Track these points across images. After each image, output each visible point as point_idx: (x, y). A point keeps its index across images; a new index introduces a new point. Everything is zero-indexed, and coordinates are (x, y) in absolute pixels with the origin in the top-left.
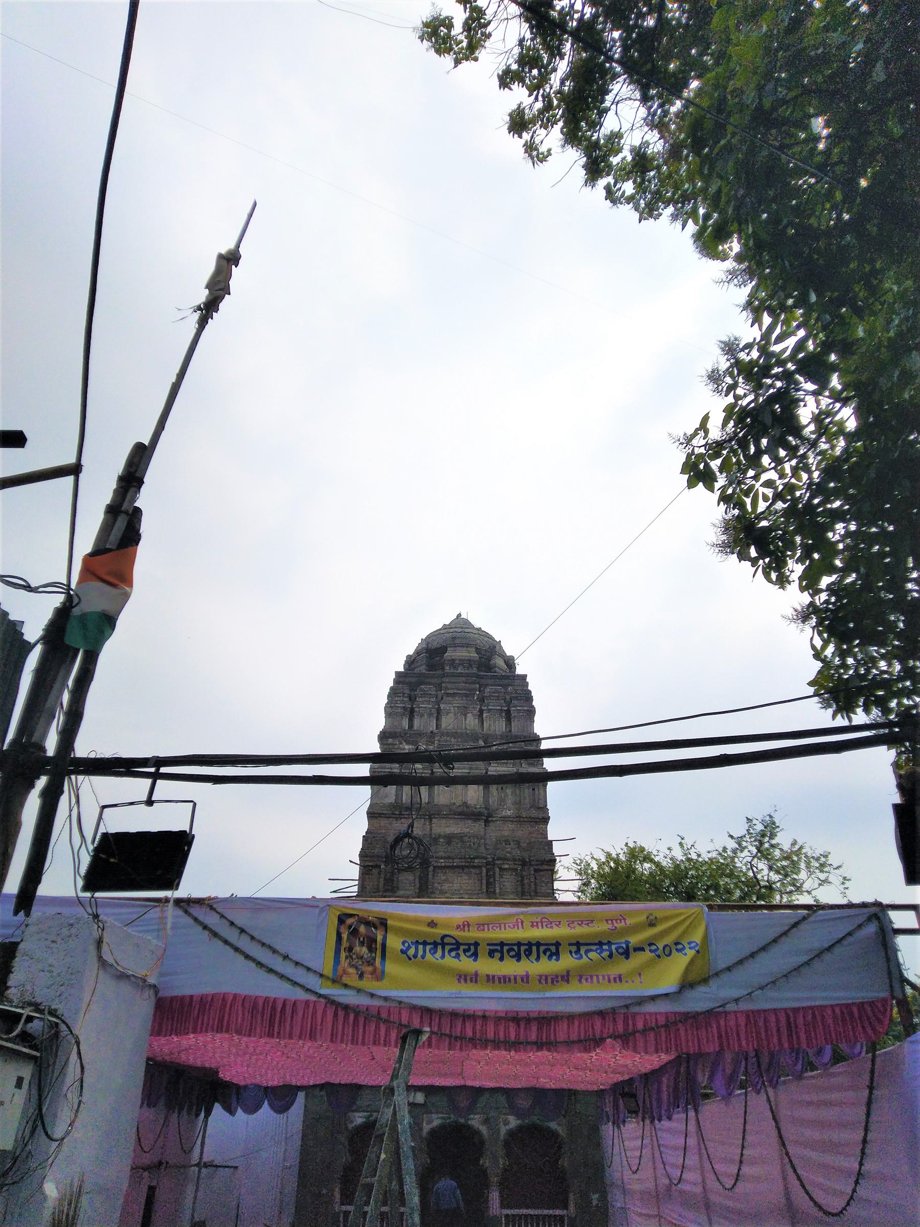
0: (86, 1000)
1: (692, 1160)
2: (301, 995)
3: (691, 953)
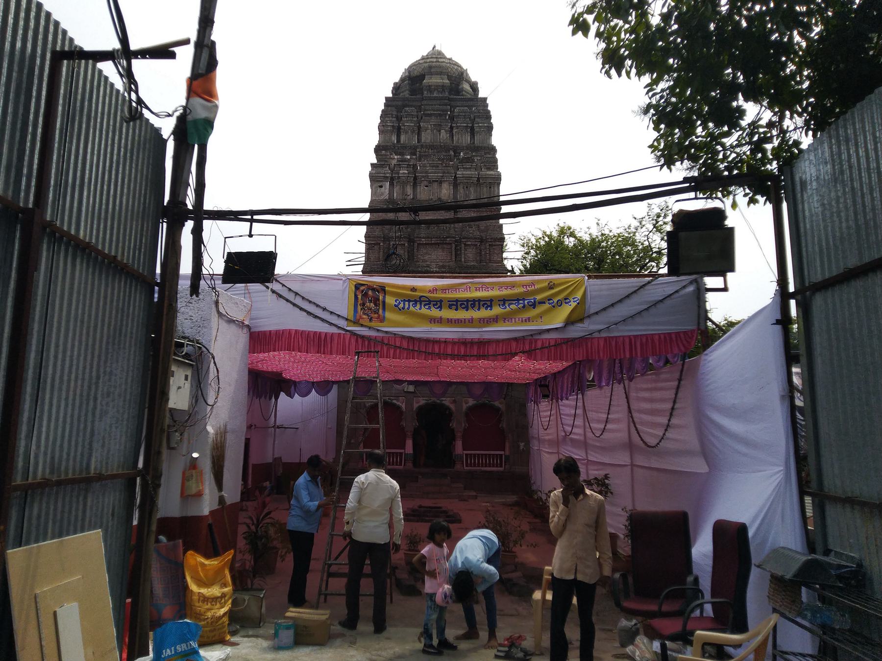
0: (214, 333)
1: (579, 422)
2: (334, 330)
3: (574, 304)
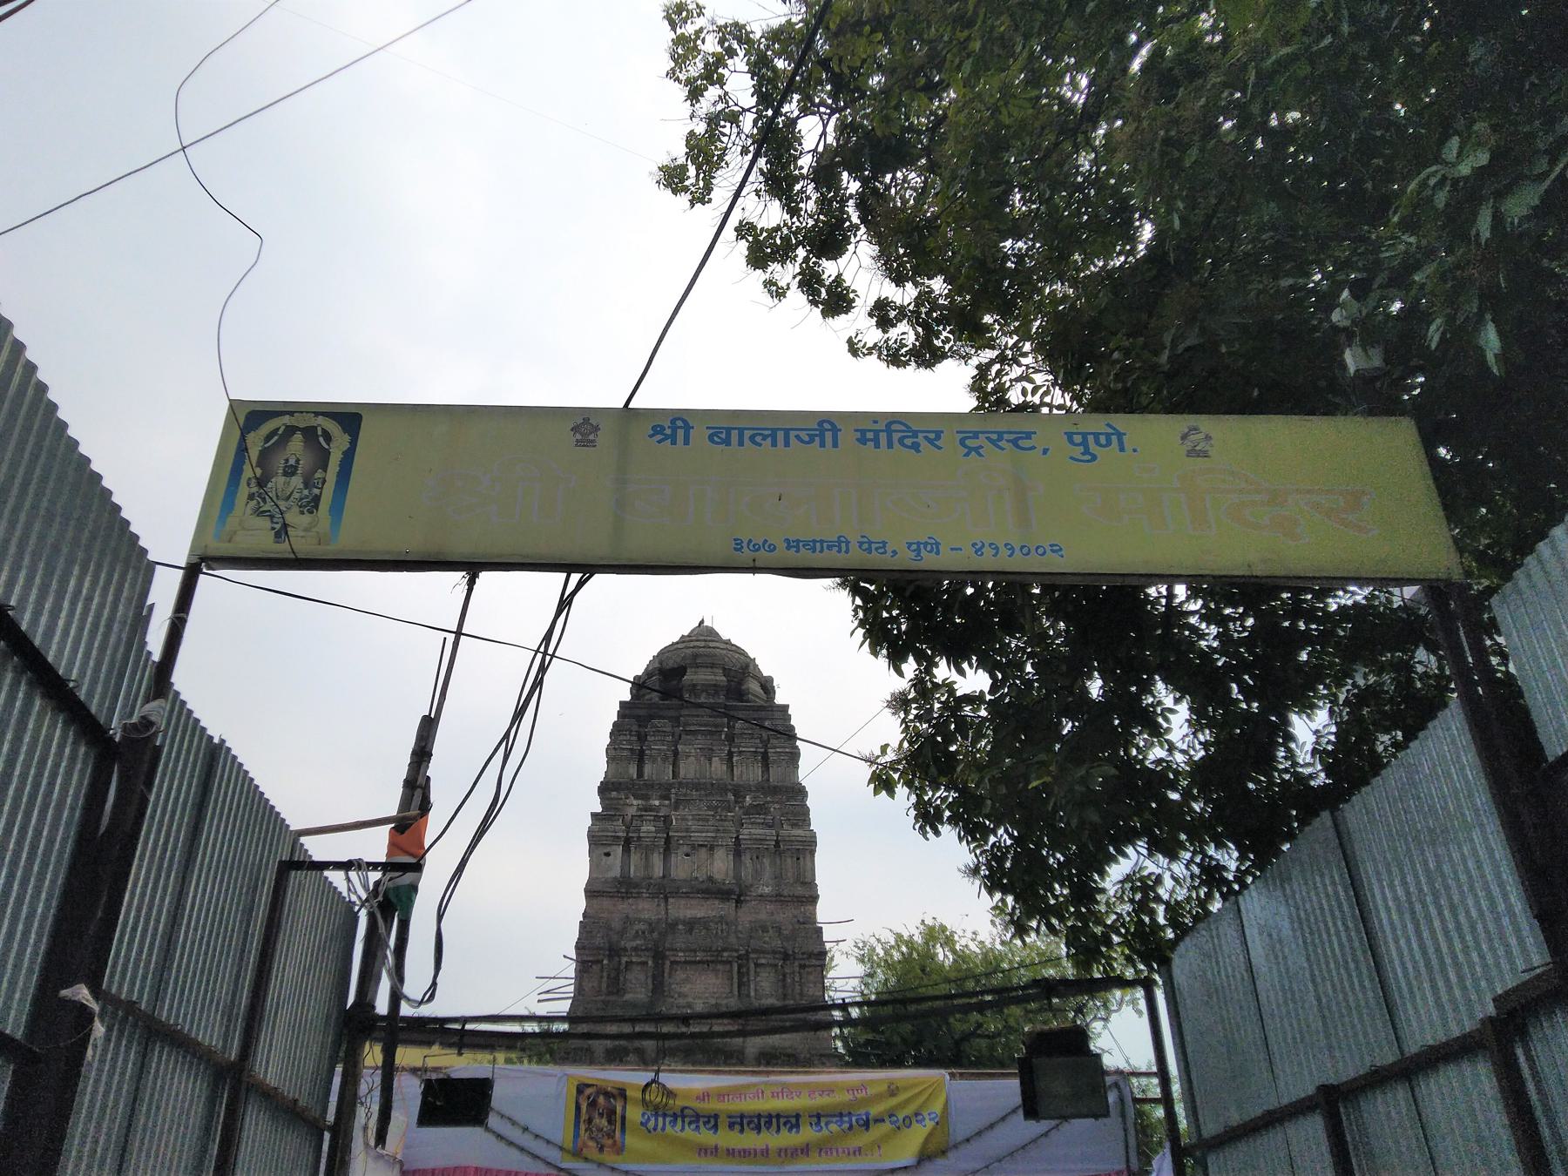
3: (930, 1124)
